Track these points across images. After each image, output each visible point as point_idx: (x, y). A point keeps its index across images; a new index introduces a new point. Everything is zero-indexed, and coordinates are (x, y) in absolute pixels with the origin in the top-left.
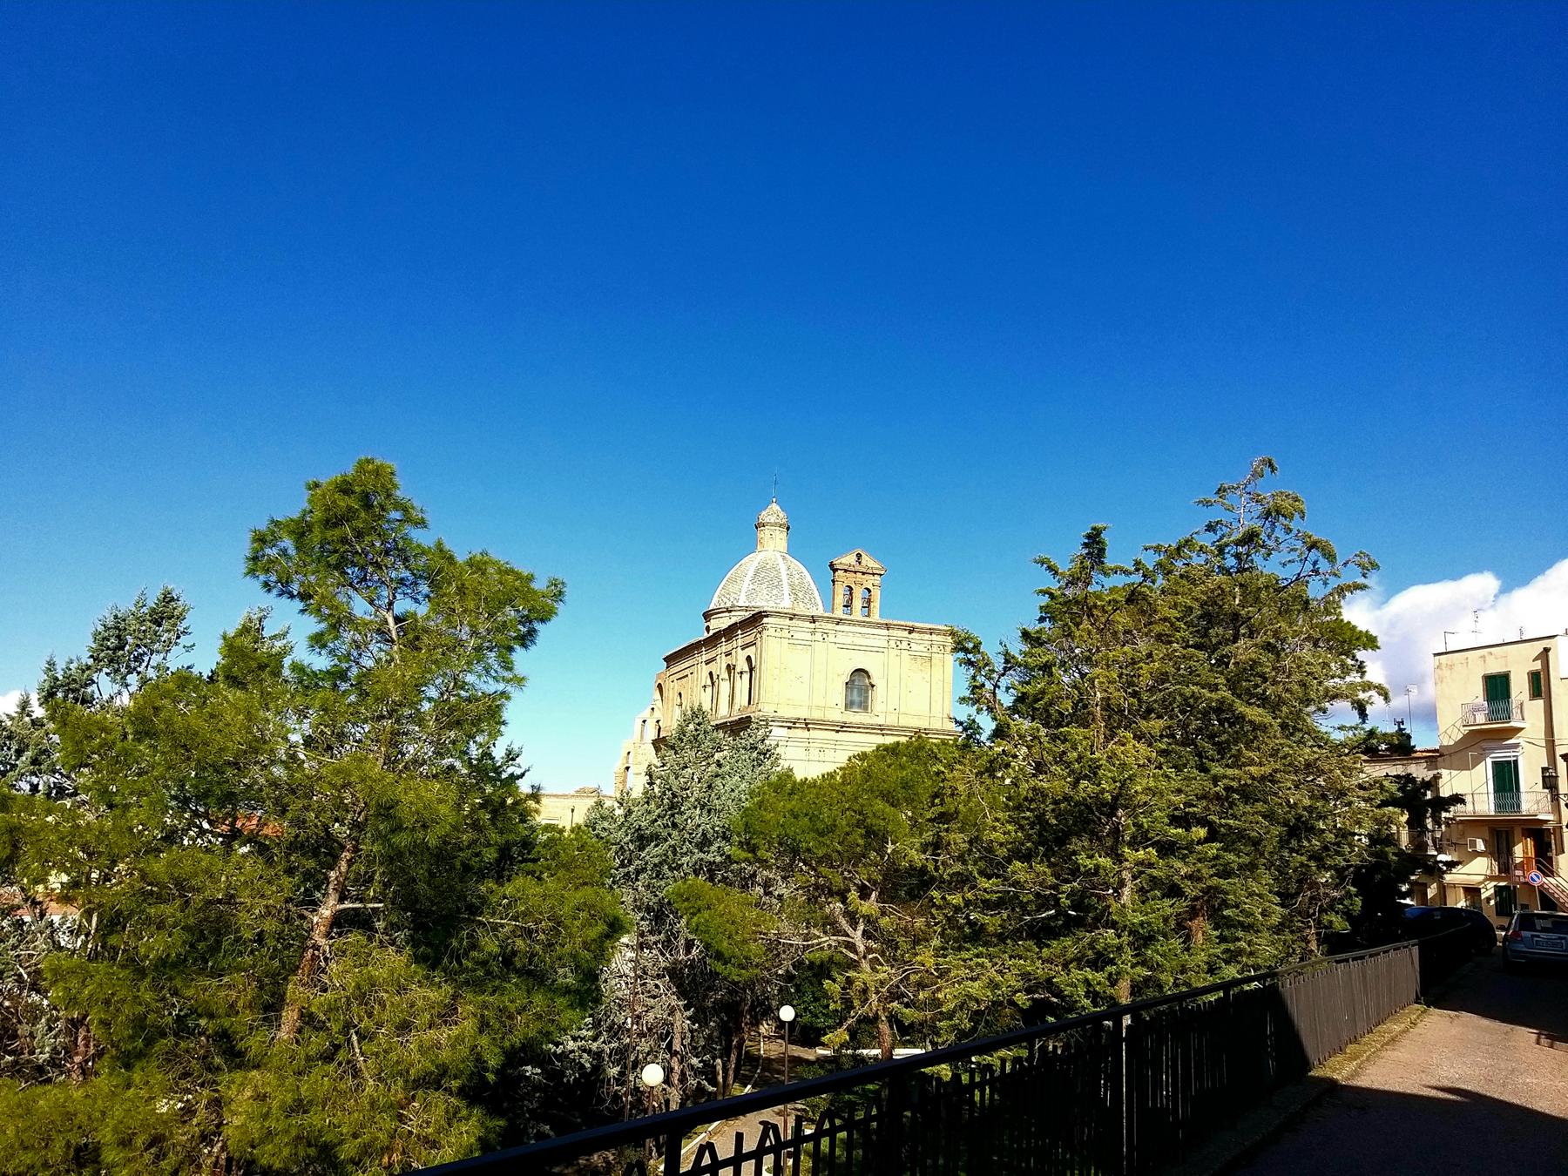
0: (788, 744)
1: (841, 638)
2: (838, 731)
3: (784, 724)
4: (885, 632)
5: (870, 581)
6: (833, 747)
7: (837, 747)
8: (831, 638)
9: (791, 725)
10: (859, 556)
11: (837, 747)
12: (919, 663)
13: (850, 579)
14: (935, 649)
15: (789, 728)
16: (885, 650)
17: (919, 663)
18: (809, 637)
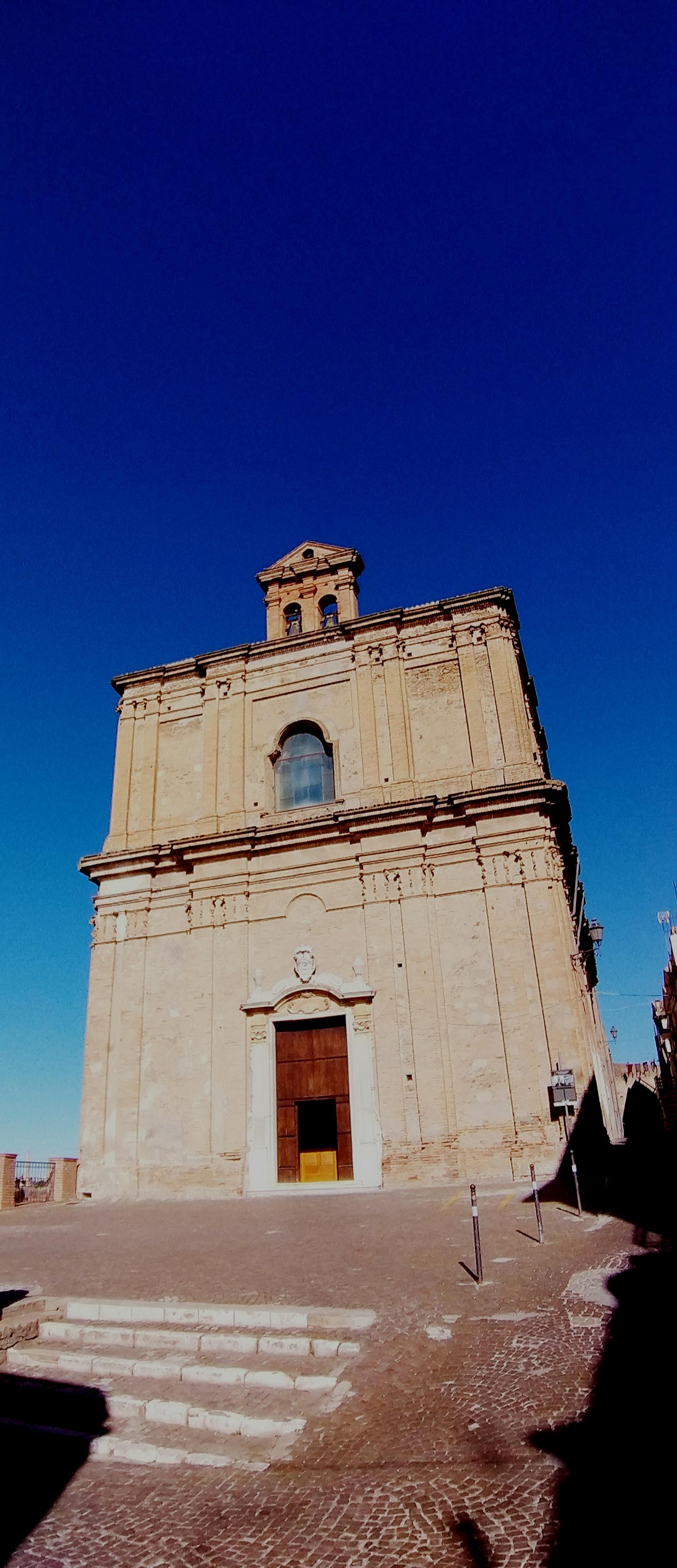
0: (152, 905)
1: (257, 682)
2: (250, 855)
3: (138, 866)
4: (344, 644)
5: (326, 586)
6: (245, 888)
7: (251, 889)
8: (238, 686)
9: (151, 864)
10: (308, 554)
11: (251, 889)
12: (434, 678)
13: (290, 594)
14: (463, 638)
15: (153, 872)
16: (352, 675)
17: (434, 678)
18: (198, 699)
